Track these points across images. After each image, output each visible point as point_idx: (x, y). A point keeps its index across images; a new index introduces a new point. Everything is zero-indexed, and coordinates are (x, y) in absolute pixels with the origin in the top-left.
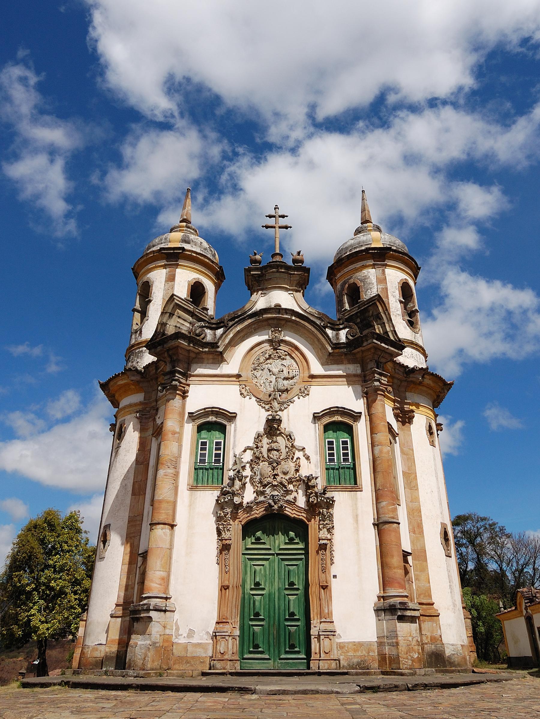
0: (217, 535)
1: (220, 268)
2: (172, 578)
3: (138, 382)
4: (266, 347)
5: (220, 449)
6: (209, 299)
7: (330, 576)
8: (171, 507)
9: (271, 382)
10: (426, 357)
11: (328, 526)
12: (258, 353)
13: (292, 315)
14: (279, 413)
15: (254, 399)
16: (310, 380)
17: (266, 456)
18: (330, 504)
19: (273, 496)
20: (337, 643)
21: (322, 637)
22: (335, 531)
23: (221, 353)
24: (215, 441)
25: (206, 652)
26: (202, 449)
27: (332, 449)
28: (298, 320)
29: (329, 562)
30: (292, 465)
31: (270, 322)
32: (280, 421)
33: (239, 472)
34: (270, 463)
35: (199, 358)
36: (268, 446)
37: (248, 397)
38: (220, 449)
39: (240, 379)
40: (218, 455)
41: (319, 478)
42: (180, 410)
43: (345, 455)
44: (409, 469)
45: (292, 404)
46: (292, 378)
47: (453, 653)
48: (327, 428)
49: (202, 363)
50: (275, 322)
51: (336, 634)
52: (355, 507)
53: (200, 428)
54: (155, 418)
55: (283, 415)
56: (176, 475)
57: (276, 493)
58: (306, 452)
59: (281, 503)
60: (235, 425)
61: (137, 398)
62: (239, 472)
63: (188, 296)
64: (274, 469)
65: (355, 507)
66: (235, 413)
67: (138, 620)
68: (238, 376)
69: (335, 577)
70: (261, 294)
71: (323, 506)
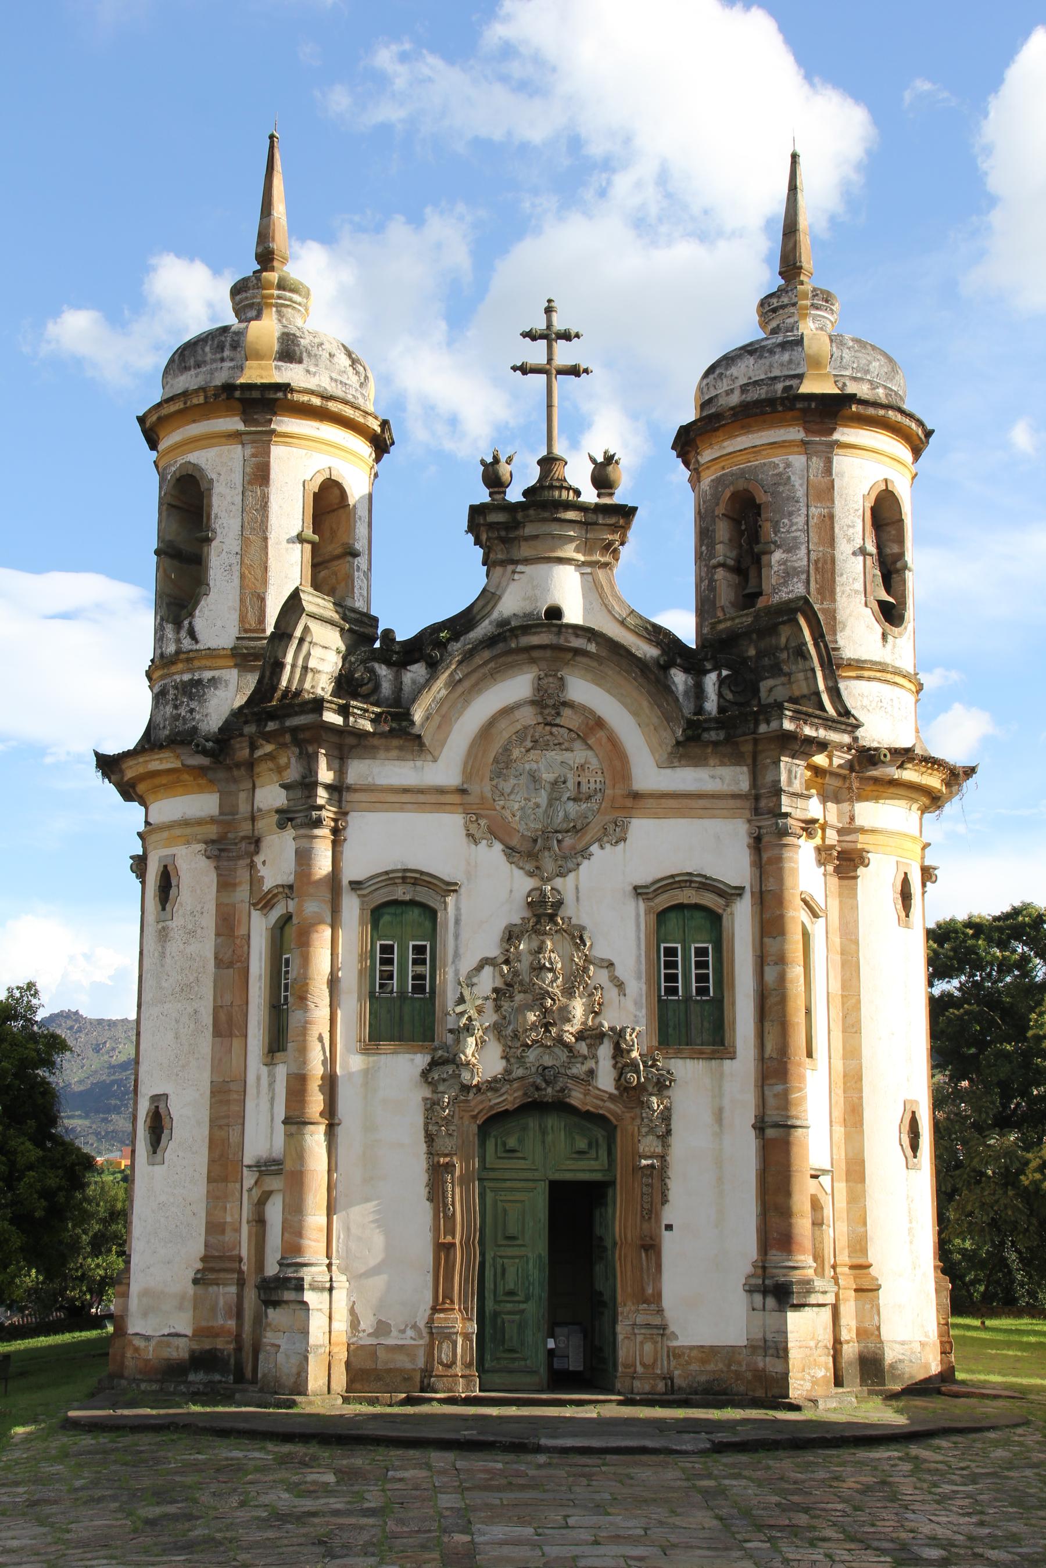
0: (425, 1145)
3: (202, 770)
4: (528, 716)
5: (423, 962)
6: (358, 524)
7: (660, 1227)
9: (538, 806)
12: (506, 735)
13: (589, 640)
15: (498, 847)
16: (629, 803)
17: (527, 980)
18: (662, 1085)
19: (545, 1068)
20: (668, 1347)
21: (639, 1338)
22: (675, 1140)
24: (411, 943)
25: (413, 1360)
28: (604, 653)
29: (658, 1198)
31: (535, 654)
35: (365, 747)
36: (531, 958)
37: (484, 842)
38: (423, 962)
39: (468, 799)
43: (702, 978)
44: (844, 987)
45: (586, 862)
46: (590, 797)
47: (901, 1357)
48: (662, 916)
49: (374, 758)
50: (548, 653)
51: (668, 1332)
52: (718, 1092)
53: (377, 915)
54: (252, 861)
57: (547, 1061)
58: (617, 973)
60: (458, 909)
62: (470, 1019)
65: (718, 1092)
66: (456, 884)
67: (276, 1304)
68: (463, 791)
69: (669, 1227)
70: (514, 572)
71: (650, 1089)
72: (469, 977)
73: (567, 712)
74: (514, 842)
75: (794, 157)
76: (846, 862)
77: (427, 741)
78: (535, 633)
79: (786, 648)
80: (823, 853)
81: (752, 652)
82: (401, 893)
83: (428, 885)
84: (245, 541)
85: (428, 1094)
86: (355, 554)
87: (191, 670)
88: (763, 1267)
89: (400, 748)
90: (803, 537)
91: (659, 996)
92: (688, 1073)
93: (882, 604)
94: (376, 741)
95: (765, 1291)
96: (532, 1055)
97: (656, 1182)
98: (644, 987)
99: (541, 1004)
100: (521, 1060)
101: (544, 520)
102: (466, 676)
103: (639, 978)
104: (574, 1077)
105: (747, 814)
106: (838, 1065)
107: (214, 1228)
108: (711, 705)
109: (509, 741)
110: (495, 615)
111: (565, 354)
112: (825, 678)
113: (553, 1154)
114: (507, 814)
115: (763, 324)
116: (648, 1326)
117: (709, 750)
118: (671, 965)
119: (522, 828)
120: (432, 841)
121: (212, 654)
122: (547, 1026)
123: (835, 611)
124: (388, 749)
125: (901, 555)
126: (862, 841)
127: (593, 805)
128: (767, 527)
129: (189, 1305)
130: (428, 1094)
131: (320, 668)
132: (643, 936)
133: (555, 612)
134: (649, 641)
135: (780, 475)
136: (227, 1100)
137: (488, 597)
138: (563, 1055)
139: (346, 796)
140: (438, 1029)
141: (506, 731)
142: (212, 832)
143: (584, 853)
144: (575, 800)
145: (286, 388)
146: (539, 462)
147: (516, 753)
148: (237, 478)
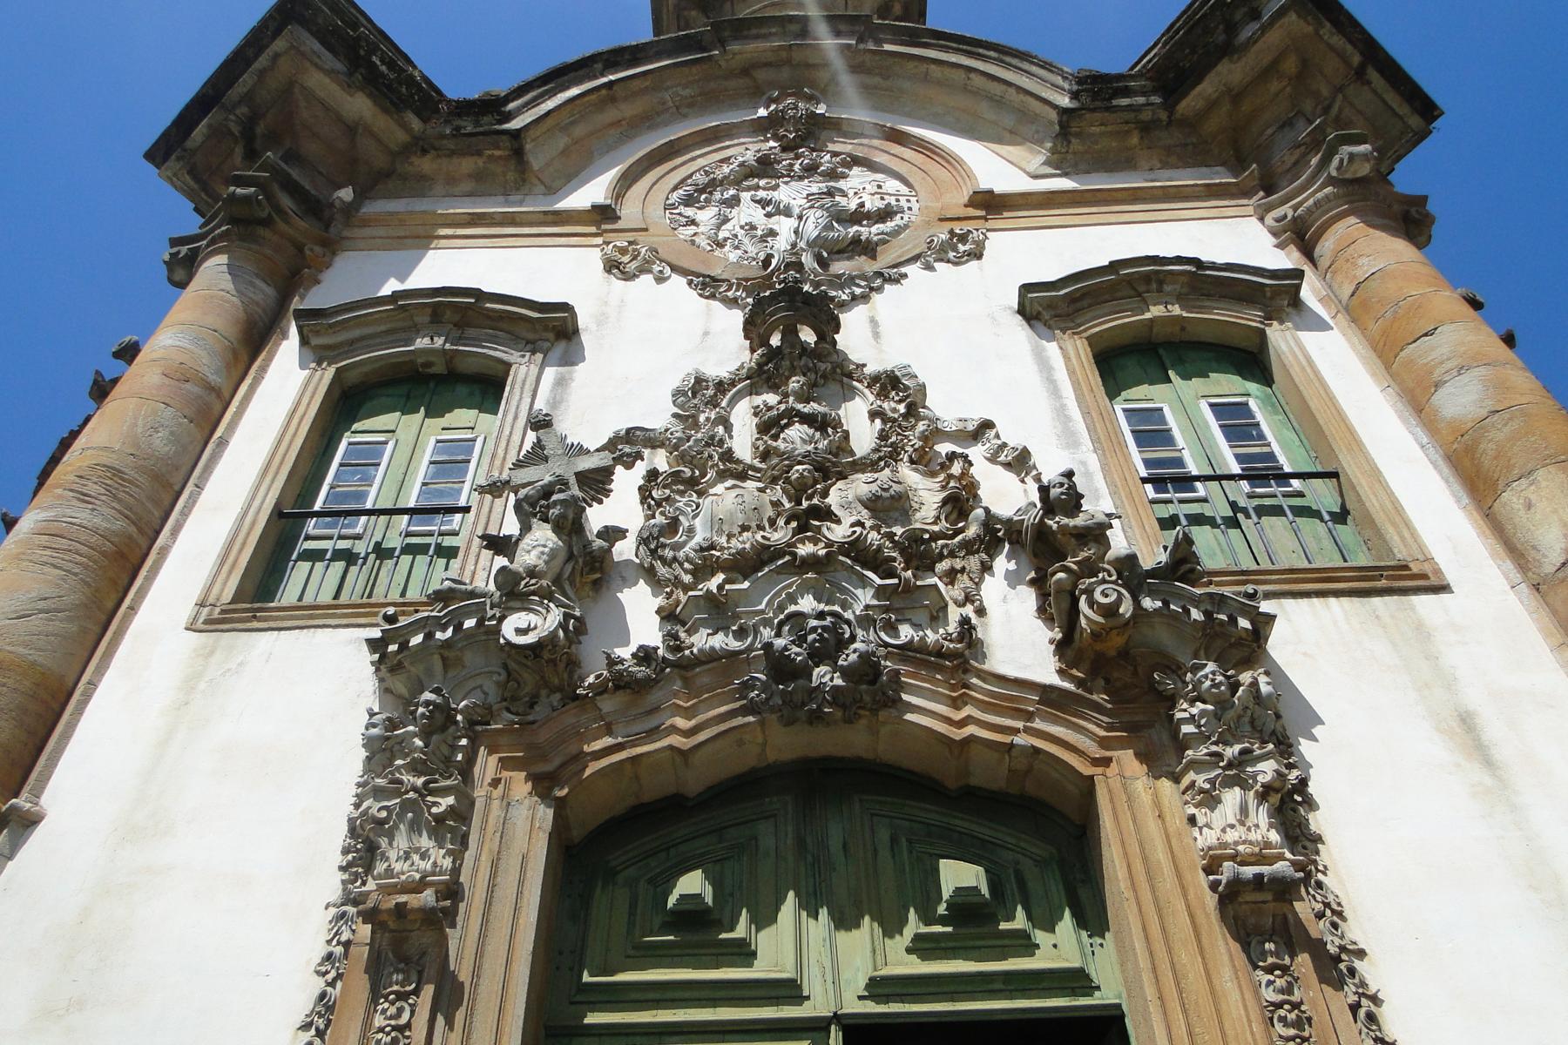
11: (1266, 770)
15: (678, 282)
31: (762, 75)
66: (565, 307)
77: (537, 158)
78: (757, 37)
89: (479, 177)
94: (426, 164)
99: (787, 481)
117: (1134, 140)
124: (451, 180)
132: (1062, 375)
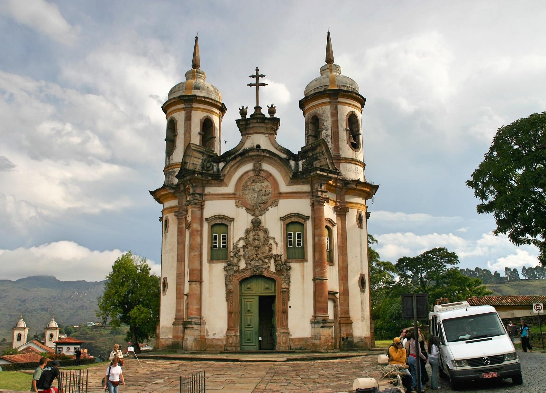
1: (223, 104)
2: (203, 308)
4: (252, 174)
5: (225, 239)
8: (199, 273)
10: (364, 166)
14: (260, 217)
15: (244, 208)
16: (278, 195)
23: (223, 180)
25: (222, 342)
26: (214, 240)
27: (291, 238)
28: (271, 156)
30: (267, 248)
32: (260, 222)
33: (236, 253)
34: (255, 247)
38: (225, 239)
40: (224, 243)
41: (282, 256)
42: (200, 217)
43: (299, 241)
46: (268, 194)
48: (288, 225)
52: (303, 271)
55: (262, 218)
56: (201, 255)
57: (257, 264)
59: (260, 270)
61: (173, 203)
62: (236, 253)
63: (201, 130)
64: (256, 251)
65: (303, 271)
67: (187, 328)
68: (234, 194)
69: (290, 307)
72: (237, 243)
73: (262, 172)
74: (248, 207)
75: (329, 33)
76: (342, 211)
77: (225, 181)
79: (319, 153)
80: (336, 209)
81: (311, 154)
82: (218, 221)
83: (225, 219)
84: (185, 134)
85: (226, 274)
86: (215, 138)
87: (172, 169)
88: (315, 317)
90: (330, 126)
91: (287, 246)
92: (295, 266)
93: (352, 143)
95: (315, 323)
96: (253, 263)
97: (286, 295)
98: (283, 244)
100: (250, 264)
101: (254, 123)
102: (235, 164)
103: (281, 241)
104: (264, 268)
105: (310, 197)
106: (341, 265)
107: (178, 311)
108: (300, 170)
109: (247, 181)
110: (242, 149)
111: (261, 80)
112: (329, 160)
113: (259, 289)
114: (246, 200)
115: (322, 74)
116: (284, 333)
118: (291, 238)
119: (250, 203)
120: (227, 208)
121: (176, 164)
122: (257, 255)
123: (338, 145)
124: (215, 184)
125: (358, 131)
126: (347, 205)
127: (269, 196)
128: (320, 125)
129: (172, 330)
130: (226, 274)
131: (197, 163)
133: (258, 146)
134: (284, 153)
135: (324, 111)
136: (180, 277)
137: (242, 143)
138: (261, 262)
139: (204, 197)
140: (229, 256)
141: (246, 178)
142: (177, 209)
143: (267, 209)
144: (264, 195)
145: (195, 95)
146: (255, 108)
147: (248, 183)
148: (183, 119)
